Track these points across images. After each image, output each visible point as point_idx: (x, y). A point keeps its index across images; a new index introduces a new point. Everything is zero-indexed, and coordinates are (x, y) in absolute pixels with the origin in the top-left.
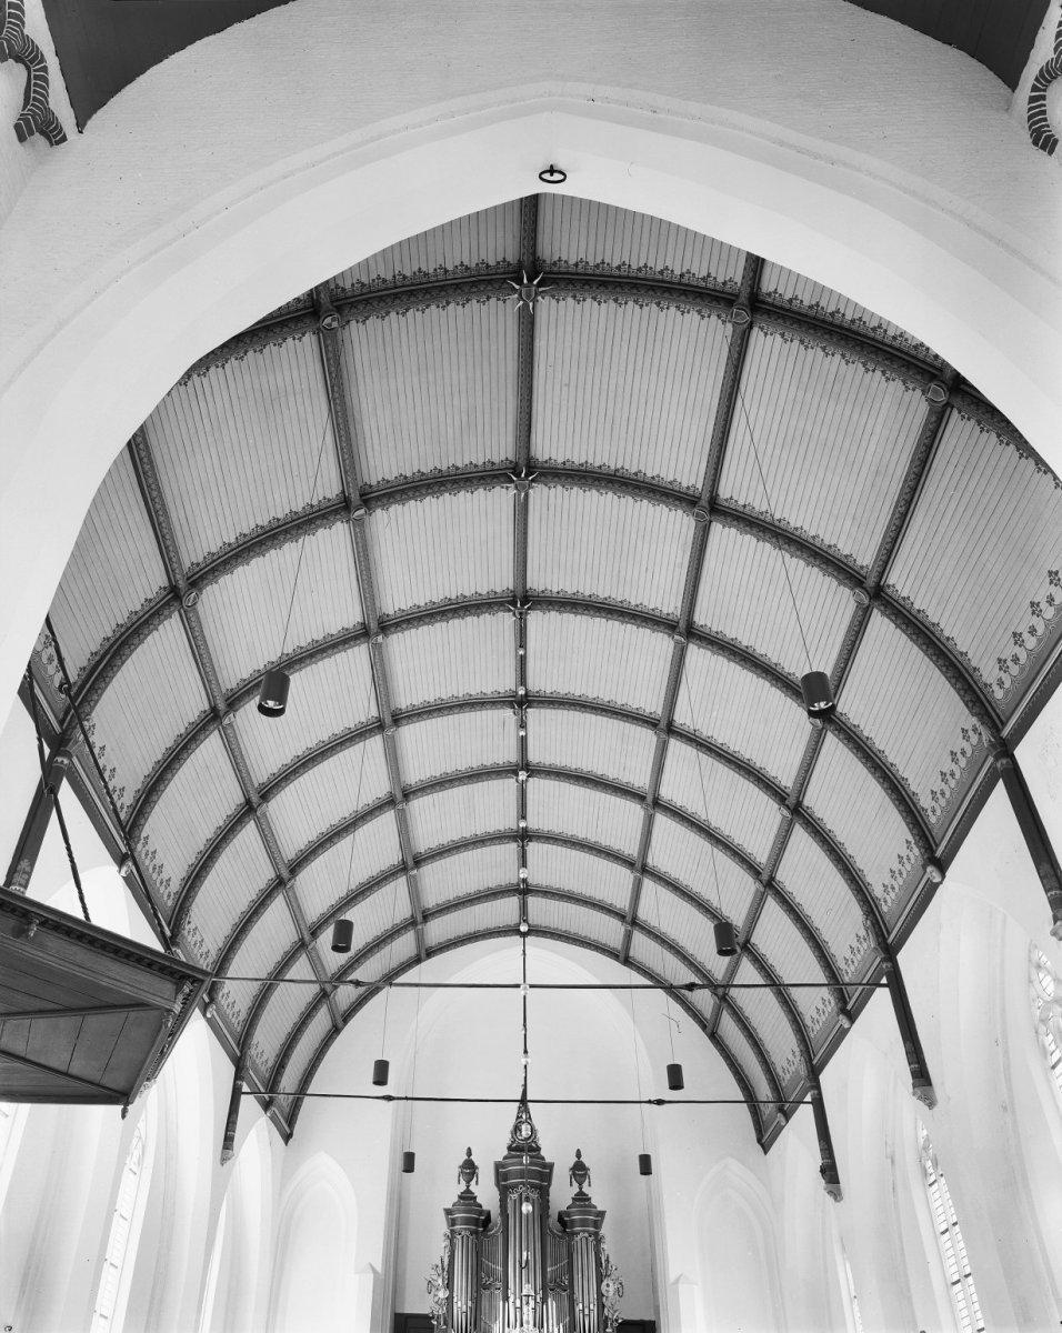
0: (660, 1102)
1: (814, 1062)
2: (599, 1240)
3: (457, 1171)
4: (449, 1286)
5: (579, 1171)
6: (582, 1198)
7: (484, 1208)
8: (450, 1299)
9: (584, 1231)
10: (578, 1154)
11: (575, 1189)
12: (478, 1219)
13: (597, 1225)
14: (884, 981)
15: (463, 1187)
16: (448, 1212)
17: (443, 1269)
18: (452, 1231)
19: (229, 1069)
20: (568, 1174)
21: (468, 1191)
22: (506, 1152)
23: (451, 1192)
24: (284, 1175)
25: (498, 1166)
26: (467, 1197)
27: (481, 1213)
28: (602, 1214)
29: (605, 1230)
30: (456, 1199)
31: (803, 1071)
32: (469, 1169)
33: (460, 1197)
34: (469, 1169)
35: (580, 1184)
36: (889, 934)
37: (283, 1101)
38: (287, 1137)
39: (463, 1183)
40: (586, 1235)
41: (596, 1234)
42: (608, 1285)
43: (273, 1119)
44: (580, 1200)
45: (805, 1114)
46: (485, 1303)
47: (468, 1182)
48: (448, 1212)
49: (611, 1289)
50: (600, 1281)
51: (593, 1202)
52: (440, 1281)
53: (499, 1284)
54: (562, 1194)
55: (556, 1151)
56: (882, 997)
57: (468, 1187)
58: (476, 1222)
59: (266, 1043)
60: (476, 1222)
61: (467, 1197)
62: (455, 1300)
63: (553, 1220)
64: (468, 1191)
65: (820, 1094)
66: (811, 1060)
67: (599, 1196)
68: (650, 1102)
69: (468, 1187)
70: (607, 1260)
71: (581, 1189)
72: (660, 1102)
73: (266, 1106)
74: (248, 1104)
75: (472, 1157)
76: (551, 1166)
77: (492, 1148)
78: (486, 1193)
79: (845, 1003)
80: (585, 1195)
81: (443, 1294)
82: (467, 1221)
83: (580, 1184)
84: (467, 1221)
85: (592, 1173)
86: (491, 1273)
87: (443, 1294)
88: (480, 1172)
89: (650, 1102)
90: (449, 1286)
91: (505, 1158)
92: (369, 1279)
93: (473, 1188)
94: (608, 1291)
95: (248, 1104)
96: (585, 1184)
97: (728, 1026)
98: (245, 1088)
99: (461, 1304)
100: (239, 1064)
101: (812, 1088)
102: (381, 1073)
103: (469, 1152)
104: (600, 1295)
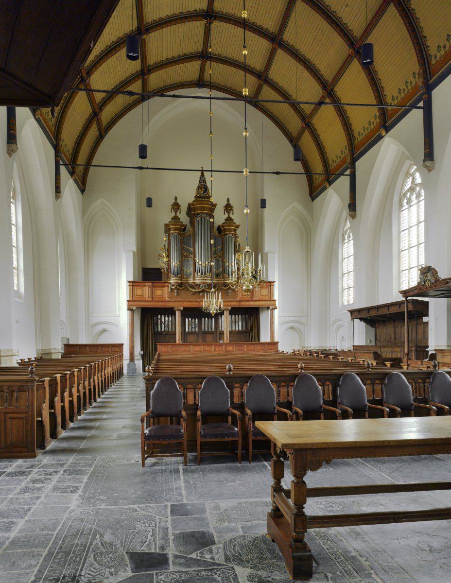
0: (278, 173)
1: (355, 156)
3: (170, 207)
4: (168, 256)
5: (228, 208)
6: (229, 219)
8: (169, 262)
10: (228, 200)
11: (226, 215)
12: (180, 228)
13: (235, 231)
14: (421, 104)
15: (173, 214)
16: (166, 225)
17: (165, 250)
19: (52, 151)
20: (222, 209)
22: (194, 199)
23: (166, 216)
24: (84, 209)
25: (189, 205)
27: (183, 225)
28: (238, 226)
29: (238, 232)
31: (349, 160)
32: (176, 206)
33: (172, 219)
34: (176, 206)
35: (229, 214)
36: (431, 78)
37: (80, 169)
38: (83, 191)
39: (173, 212)
43: (75, 181)
44: (229, 220)
45: (344, 182)
46: (185, 263)
47: (176, 212)
48: (166, 225)
51: (235, 221)
52: (164, 254)
53: (192, 256)
54: (219, 217)
55: (218, 197)
56: (416, 116)
57: (176, 214)
58: (180, 230)
59: (69, 136)
60: (180, 230)
61: (176, 219)
62: (172, 262)
63: (215, 229)
65: (355, 171)
66: (353, 154)
68: (274, 173)
70: (239, 245)
72: (278, 173)
73: (72, 173)
74: (63, 169)
76: (215, 205)
77: (188, 195)
79: (385, 123)
81: (165, 260)
82: (175, 229)
83: (229, 214)
85: (234, 209)
86: (187, 251)
87: (165, 260)
89: (274, 173)
90: (168, 256)
91: (193, 201)
92: (131, 254)
93: (178, 214)
95: (63, 169)
96: (231, 214)
97: (307, 140)
98: (61, 163)
99: (174, 263)
100: (57, 147)
101: (350, 168)
102: (143, 152)
103: (176, 199)
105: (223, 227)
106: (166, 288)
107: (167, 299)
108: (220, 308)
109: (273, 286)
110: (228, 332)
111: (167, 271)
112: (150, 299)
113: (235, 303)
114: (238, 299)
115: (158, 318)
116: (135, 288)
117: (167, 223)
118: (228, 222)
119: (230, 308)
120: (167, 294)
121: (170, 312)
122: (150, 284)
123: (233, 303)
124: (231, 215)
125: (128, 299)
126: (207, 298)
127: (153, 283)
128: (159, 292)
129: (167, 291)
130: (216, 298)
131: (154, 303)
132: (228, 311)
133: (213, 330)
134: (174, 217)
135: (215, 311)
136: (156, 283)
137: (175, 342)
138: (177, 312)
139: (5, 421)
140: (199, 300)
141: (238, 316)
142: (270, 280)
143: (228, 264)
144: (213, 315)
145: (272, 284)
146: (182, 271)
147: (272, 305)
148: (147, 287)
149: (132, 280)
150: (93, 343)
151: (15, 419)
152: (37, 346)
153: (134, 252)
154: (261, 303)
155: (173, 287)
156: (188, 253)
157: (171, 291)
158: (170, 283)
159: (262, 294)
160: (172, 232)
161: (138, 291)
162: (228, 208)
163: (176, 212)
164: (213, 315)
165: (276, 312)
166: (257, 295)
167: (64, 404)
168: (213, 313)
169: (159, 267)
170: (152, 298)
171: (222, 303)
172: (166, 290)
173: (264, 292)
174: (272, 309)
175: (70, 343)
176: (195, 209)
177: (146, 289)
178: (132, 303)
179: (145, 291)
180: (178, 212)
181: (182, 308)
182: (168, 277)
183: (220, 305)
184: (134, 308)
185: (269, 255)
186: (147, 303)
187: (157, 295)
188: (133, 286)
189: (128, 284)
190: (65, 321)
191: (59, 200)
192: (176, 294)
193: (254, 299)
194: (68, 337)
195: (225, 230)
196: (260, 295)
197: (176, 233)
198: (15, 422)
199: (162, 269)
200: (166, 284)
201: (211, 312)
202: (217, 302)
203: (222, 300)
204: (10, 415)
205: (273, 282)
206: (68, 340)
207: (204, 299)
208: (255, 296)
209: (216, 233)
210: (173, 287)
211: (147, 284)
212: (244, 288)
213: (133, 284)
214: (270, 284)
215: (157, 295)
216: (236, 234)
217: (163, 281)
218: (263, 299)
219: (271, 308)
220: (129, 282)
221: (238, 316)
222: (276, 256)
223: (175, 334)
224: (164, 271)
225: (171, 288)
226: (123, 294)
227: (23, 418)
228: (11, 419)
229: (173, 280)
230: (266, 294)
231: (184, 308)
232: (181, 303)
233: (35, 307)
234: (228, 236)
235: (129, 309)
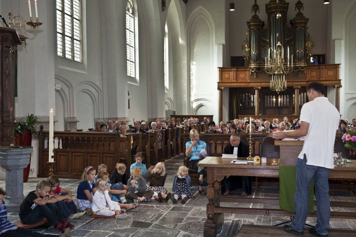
2: (306, 28)
3: (251, 8)
4: (250, 47)
5: (299, 5)
6: (300, 15)
7: (262, 20)
8: (250, 51)
9: (300, 26)
11: (297, 11)
13: (306, 23)
15: (253, 13)
16: (248, 23)
17: (247, 42)
18: (250, 29)
20: (294, 6)
21: (255, 15)
23: (249, 16)
24: (186, 15)
25: (266, 5)
26: (255, 17)
27: (261, 22)
28: (308, 19)
29: (308, 25)
30: (251, 18)
32: (256, 7)
33: (253, 17)
34: (256, 7)
40: (301, 27)
41: (305, 27)
42: (308, 44)
46: (263, 52)
47: (255, 12)
48: (248, 23)
49: (310, 45)
50: (305, 42)
52: (246, 46)
54: (292, 13)
57: (255, 14)
61: (255, 17)
62: (252, 51)
64: (255, 15)
67: (306, 12)
69: (255, 14)
70: (309, 35)
71: (299, 11)
75: (257, 3)
76: (288, 4)
78: (262, 15)
80: (301, 13)
82: (254, 25)
84: (254, 25)
85: (304, 5)
86: (265, 42)
88: (260, 8)
90: (250, 47)
91: (270, 2)
92: (221, 47)
93: (257, 13)
94: (308, 45)
96: (301, 10)
104: (305, 46)
105: (294, 20)
106: (248, 72)
107: (248, 81)
108: (284, 87)
109: (339, 67)
110: (299, 107)
111: (249, 58)
112: (235, 81)
113: (304, 83)
114: (307, 79)
115: (245, 95)
116: (224, 73)
117: (249, 21)
118: (298, 16)
119: (299, 87)
120: (248, 77)
121: (251, 91)
122: (235, 69)
123: (302, 83)
124: (301, 11)
125: (218, 81)
126: (274, 79)
127: (237, 69)
128: (242, 75)
129: (248, 74)
130: (281, 79)
131: (238, 84)
132: (298, 90)
133: (274, 106)
134: (254, 15)
135: (280, 90)
136: (239, 68)
137: (255, 114)
138: (256, 91)
139: (103, 158)
140: (268, 81)
141: (304, 94)
142: (336, 62)
143: (298, 51)
144: (278, 93)
145: (338, 66)
146: (260, 58)
147: (337, 84)
148: (233, 72)
149: (221, 66)
150: (189, 115)
151: (108, 157)
152: (148, 116)
153: (223, 45)
154: (327, 82)
155: (253, 71)
156: (265, 44)
157: (251, 75)
158: (250, 68)
159: (328, 75)
160: (252, 28)
161: (226, 75)
162: (299, 5)
163: (255, 12)
164: (278, 93)
165: (342, 91)
166: (324, 76)
167: (146, 152)
168: (279, 91)
169: (242, 55)
170: (237, 81)
171: (286, 83)
172: (248, 73)
173: (331, 73)
174: (337, 87)
175: (176, 115)
176: (270, 9)
177: (232, 73)
178: (221, 84)
179: (231, 75)
180: (257, 12)
181: (260, 88)
182: (249, 63)
183: (284, 85)
184: (223, 88)
185: (336, 41)
186: (233, 84)
187: (241, 77)
188: (222, 71)
189: (218, 69)
190: (172, 99)
191: (165, 12)
192: (255, 77)
193: (322, 79)
194: (175, 110)
195: (296, 23)
196: (327, 76)
197: (255, 28)
198: (108, 159)
199: (244, 57)
200: (248, 69)
201: (277, 90)
202: (282, 82)
203: (286, 81)
204: (106, 155)
205: (340, 64)
206: (174, 112)
207: (271, 80)
208: (322, 77)
209: (290, 26)
210: (253, 71)
211: (232, 69)
212: (276, 72)
213: (222, 70)
214: (336, 67)
215: (241, 77)
216: (305, 26)
217: (245, 67)
218: (330, 79)
219: (336, 86)
220: (219, 68)
221: (304, 94)
222: (343, 42)
223: (255, 109)
224: (246, 59)
225: (251, 72)
226: (216, 78)
227: (112, 157)
228: (106, 157)
229: (253, 66)
230: (332, 75)
231: (262, 88)
232: (259, 84)
233: (147, 89)
234: (298, 28)
235: (219, 89)
